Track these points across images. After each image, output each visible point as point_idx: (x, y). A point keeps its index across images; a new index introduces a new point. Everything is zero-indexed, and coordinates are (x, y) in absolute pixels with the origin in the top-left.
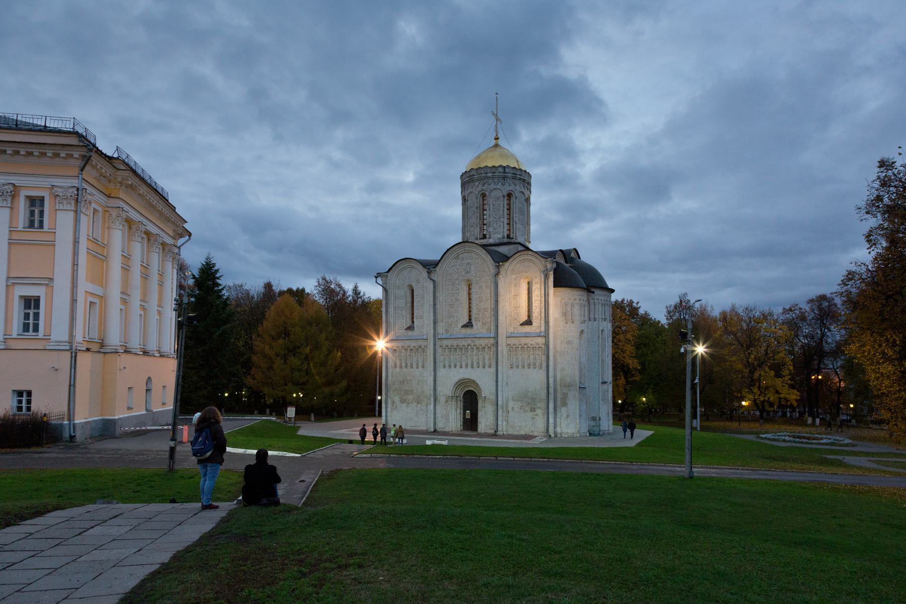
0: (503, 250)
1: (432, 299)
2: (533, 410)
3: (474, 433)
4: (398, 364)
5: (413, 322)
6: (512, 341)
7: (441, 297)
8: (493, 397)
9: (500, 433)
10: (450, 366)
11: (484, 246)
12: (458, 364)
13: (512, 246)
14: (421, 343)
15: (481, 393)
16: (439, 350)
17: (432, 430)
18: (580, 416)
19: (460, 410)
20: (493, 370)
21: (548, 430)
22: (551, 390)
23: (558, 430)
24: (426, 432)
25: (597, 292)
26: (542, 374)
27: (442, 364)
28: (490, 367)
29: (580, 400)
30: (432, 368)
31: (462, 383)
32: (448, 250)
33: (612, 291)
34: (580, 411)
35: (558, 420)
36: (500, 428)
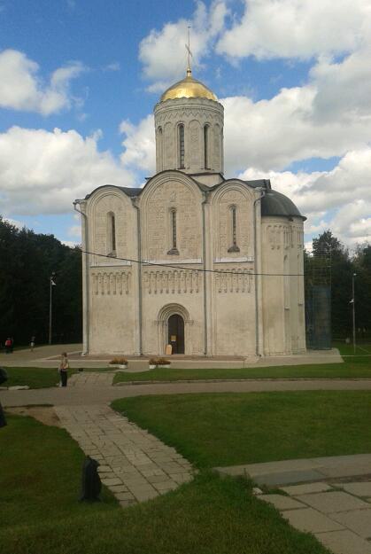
0: (203, 180)
1: (136, 226)
2: (243, 331)
4: (100, 291)
5: (114, 248)
7: (144, 225)
8: (202, 321)
9: (209, 354)
10: (156, 292)
12: (165, 290)
15: (188, 316)
16: (145, 277)
17: (139, 354)
19: (166, 335)
20: (202, 293)
21: (257, 350)
22: (260, 312)
23: (267, 349)
24: (133, 357)
25: (295, 220)
26: (250, 298)
27: (147, 290)
29: (286, 321)
33: (305, 219)
35: (266, 340)
36: (209, 350)
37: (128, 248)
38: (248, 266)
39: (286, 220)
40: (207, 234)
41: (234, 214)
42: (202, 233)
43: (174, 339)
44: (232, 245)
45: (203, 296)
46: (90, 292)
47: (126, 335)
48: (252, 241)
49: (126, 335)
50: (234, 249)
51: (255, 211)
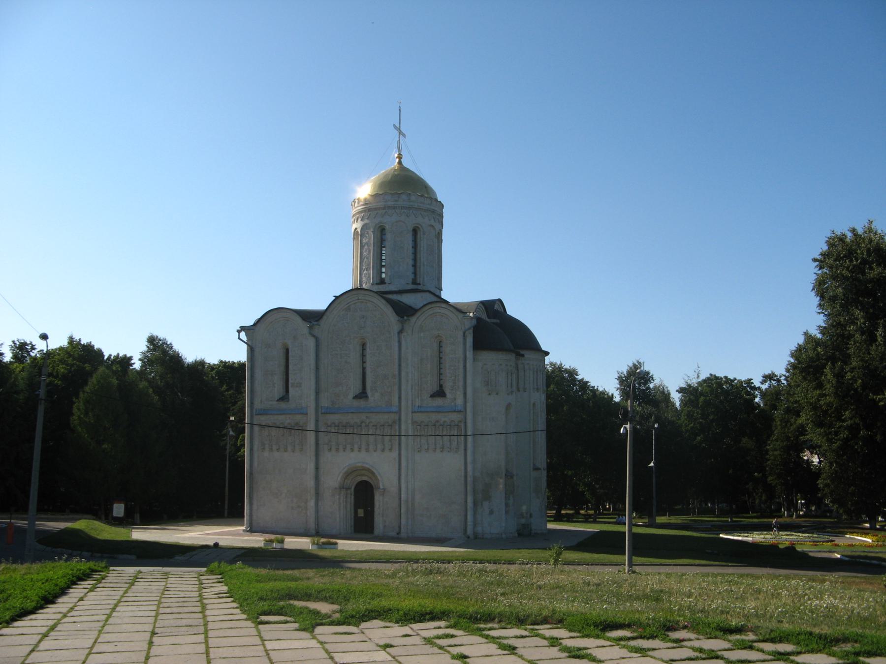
0: (408, 299)
3: (368, 536)
5: (287, 391)
6: (420, 417)
10: (337, 450)
11: (382, 294)
13: (419, 295)
14: (298, 418)
18: (507, 512)
19: (350, 507)
22: (469, 479)
23: (479, 529)
28: (391, 450)
30: (313, 453)
31: (351, 472)
32: (337, 298)
33: (547, 353)
34: (507, 505)
36: (402, 530)
37: (304, 392)
38: (455, 417)
39: (512, 357)
40: (403, 374)
41: (440, 347)
42: (397, 373)
43: (361, 513)
44: (436, 388)
45: (397, 459)
46: (255, 448)
47: (299, 507)
48: (461, 383)
49: (299, 507)
50: (440, 393)
51: (465, 344)
